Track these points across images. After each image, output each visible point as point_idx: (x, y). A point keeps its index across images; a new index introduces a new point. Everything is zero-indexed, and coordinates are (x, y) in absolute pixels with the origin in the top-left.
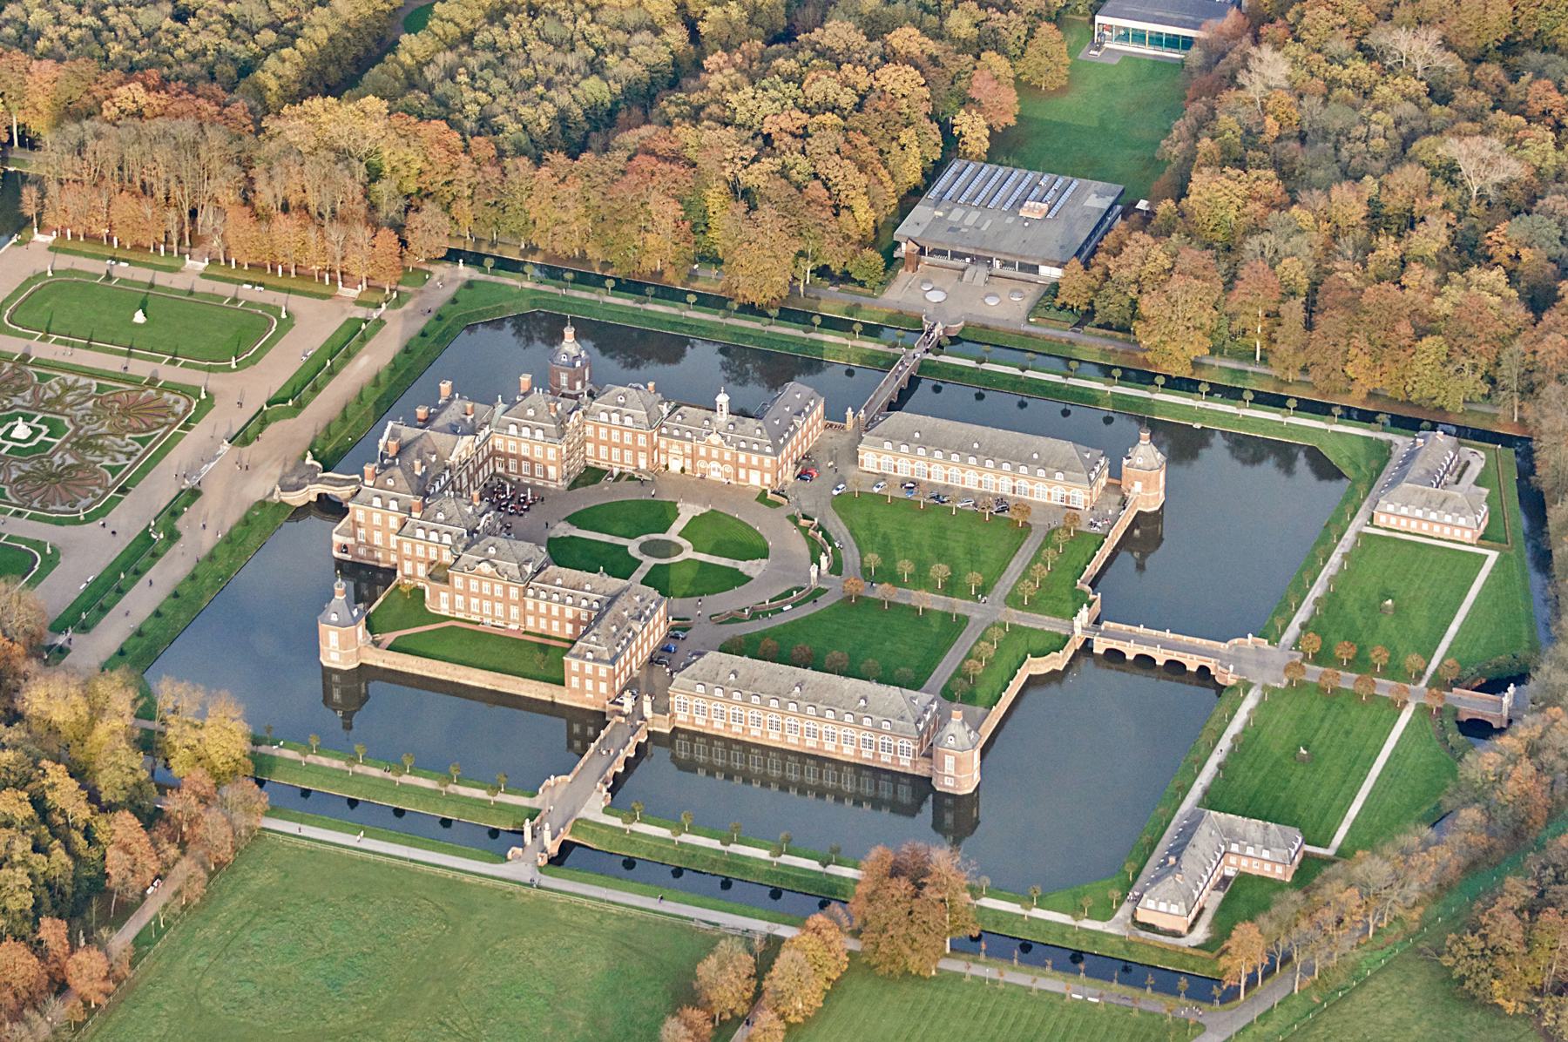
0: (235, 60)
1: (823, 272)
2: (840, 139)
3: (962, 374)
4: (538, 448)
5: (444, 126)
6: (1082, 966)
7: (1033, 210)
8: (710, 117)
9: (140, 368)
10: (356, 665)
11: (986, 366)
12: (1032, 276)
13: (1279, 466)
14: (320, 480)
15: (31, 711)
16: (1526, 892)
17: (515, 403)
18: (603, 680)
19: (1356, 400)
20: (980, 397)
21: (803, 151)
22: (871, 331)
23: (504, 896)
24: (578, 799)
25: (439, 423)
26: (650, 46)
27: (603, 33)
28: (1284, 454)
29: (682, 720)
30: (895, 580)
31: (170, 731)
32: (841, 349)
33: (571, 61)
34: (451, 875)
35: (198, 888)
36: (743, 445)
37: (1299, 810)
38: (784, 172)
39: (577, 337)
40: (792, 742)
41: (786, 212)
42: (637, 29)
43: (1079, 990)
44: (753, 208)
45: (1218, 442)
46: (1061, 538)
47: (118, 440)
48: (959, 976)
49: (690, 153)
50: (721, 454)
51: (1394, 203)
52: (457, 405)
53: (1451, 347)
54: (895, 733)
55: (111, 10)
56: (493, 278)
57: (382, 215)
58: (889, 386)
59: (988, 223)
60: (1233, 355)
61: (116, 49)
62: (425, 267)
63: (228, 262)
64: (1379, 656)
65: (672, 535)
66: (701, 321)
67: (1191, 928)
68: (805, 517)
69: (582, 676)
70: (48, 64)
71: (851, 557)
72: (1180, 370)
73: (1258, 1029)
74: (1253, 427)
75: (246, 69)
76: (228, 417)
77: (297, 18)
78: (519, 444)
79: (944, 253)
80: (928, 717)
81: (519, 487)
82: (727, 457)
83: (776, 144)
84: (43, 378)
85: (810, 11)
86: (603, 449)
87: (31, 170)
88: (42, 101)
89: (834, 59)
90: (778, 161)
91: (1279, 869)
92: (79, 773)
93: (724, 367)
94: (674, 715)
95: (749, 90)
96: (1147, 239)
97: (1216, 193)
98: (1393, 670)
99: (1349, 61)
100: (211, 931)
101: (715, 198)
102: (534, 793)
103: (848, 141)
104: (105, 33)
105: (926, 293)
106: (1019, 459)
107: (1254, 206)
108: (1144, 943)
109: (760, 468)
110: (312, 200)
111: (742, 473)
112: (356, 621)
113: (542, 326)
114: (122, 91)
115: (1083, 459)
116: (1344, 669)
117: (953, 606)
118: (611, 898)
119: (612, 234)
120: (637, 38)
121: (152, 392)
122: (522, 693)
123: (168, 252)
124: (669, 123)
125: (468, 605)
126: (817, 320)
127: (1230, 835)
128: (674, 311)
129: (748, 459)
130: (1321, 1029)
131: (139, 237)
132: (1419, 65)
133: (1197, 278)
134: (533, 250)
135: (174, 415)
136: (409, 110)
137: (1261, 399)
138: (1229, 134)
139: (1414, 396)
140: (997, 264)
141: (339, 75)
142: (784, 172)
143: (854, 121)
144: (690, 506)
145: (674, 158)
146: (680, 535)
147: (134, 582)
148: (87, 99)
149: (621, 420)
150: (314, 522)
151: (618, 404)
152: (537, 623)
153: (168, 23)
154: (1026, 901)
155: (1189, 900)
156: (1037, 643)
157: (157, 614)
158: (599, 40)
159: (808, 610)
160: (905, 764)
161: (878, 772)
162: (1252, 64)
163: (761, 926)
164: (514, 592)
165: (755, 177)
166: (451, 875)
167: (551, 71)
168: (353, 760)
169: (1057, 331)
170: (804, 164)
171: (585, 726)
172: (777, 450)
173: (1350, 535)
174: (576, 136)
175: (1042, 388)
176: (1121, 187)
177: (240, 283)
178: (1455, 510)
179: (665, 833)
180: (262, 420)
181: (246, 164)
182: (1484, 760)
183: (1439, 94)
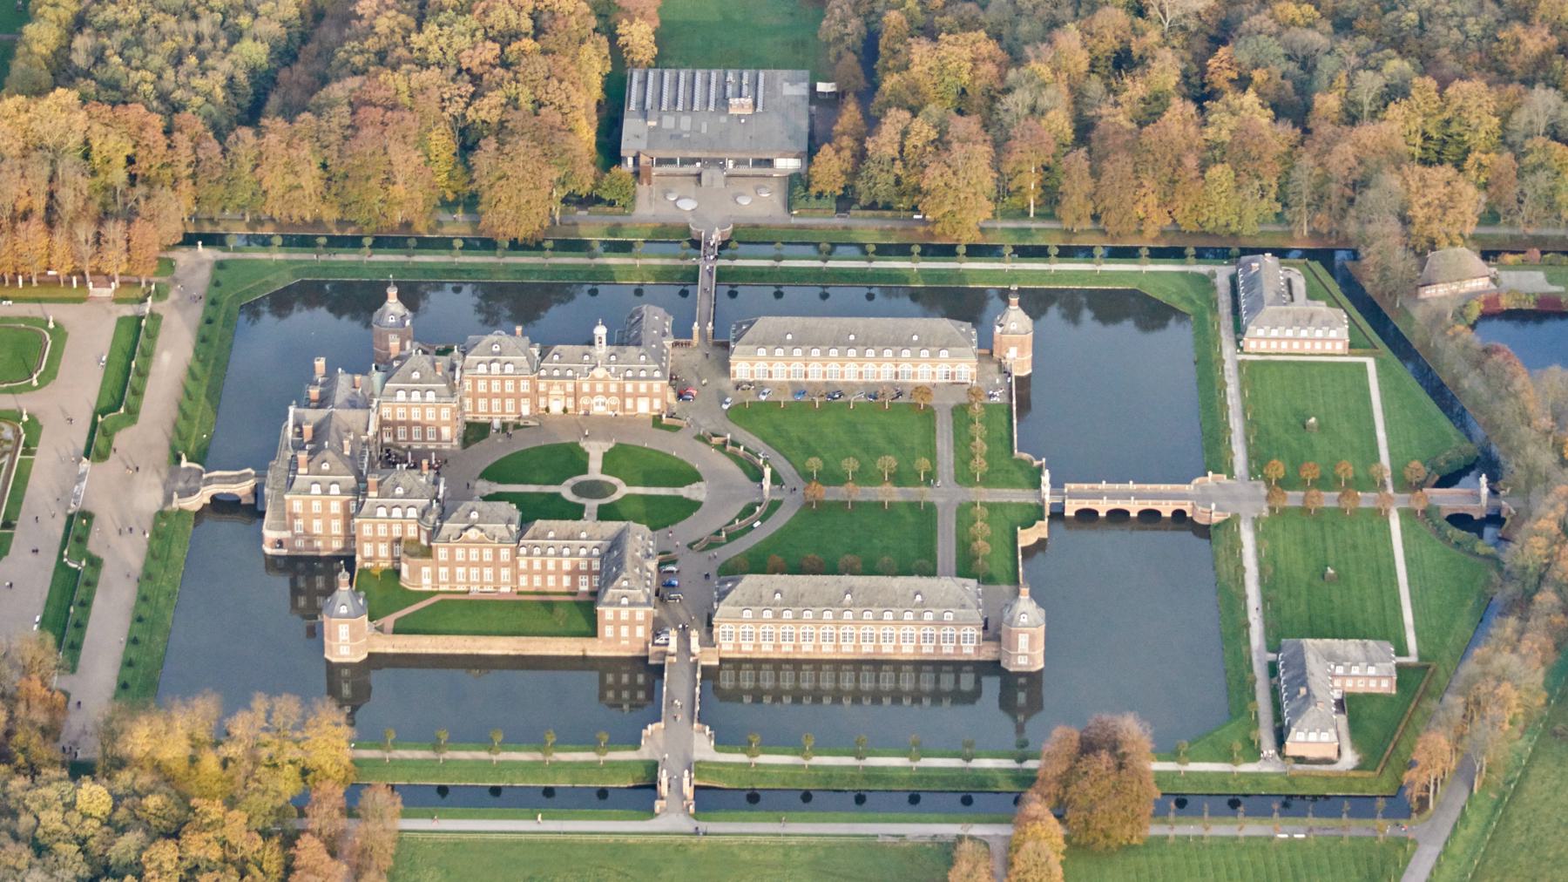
3: (762, 275)
6: (1241, 809)
7: (740, 106)
11: (785, 263)
13: (1064, 316)
14: (209, 482)
15: (138, 752)
20: (779, 295)
23: (673, 851)
24: (680, 745)
29: (727, 648)
32: (630, 270)
33: (205, 26)
34: (612, 839)
37: (1359, 625)
38: (513, 103)
39: (400, 297)
40: (848, 650)
43: (1285, 831)
49: (404, 98)
50: (606, 387)
51: (1109, 44)
52: (343, 379)
54: (957, 624)
56: (239, 255)
60: (1006, 215)
62: (163, 255)
64: (1346, 469)
69: (617, 623)
72: (970, 237)
73: (1463, 832)
74: (1069, 281)
78: (409, 409)
79: (672, 161)
86: (482, 402)
98: (1356, 484)
102: (636, 744)
106: (900, 343)
109: (650, 395)
111: (629, 403)
127: (1332, 657)
129: (636, 388)
130: (1517, 823)
135: (9, 442)
137: (1066, 253)
140: (730, 164)
142: (513, 103)
143: (549, 40)
144: (593, 443)
145: (394, 107)
147: (87, 615)
151: (493, 354)
152: (530, 581)
154: (1174, 756)
157: (134, 641)
160: (969, 651)
161: (938, 666)
164: (505, 554)
165: (488, 109)
169: (826, 220)
176: (807, 73)
178: (1325, 323)
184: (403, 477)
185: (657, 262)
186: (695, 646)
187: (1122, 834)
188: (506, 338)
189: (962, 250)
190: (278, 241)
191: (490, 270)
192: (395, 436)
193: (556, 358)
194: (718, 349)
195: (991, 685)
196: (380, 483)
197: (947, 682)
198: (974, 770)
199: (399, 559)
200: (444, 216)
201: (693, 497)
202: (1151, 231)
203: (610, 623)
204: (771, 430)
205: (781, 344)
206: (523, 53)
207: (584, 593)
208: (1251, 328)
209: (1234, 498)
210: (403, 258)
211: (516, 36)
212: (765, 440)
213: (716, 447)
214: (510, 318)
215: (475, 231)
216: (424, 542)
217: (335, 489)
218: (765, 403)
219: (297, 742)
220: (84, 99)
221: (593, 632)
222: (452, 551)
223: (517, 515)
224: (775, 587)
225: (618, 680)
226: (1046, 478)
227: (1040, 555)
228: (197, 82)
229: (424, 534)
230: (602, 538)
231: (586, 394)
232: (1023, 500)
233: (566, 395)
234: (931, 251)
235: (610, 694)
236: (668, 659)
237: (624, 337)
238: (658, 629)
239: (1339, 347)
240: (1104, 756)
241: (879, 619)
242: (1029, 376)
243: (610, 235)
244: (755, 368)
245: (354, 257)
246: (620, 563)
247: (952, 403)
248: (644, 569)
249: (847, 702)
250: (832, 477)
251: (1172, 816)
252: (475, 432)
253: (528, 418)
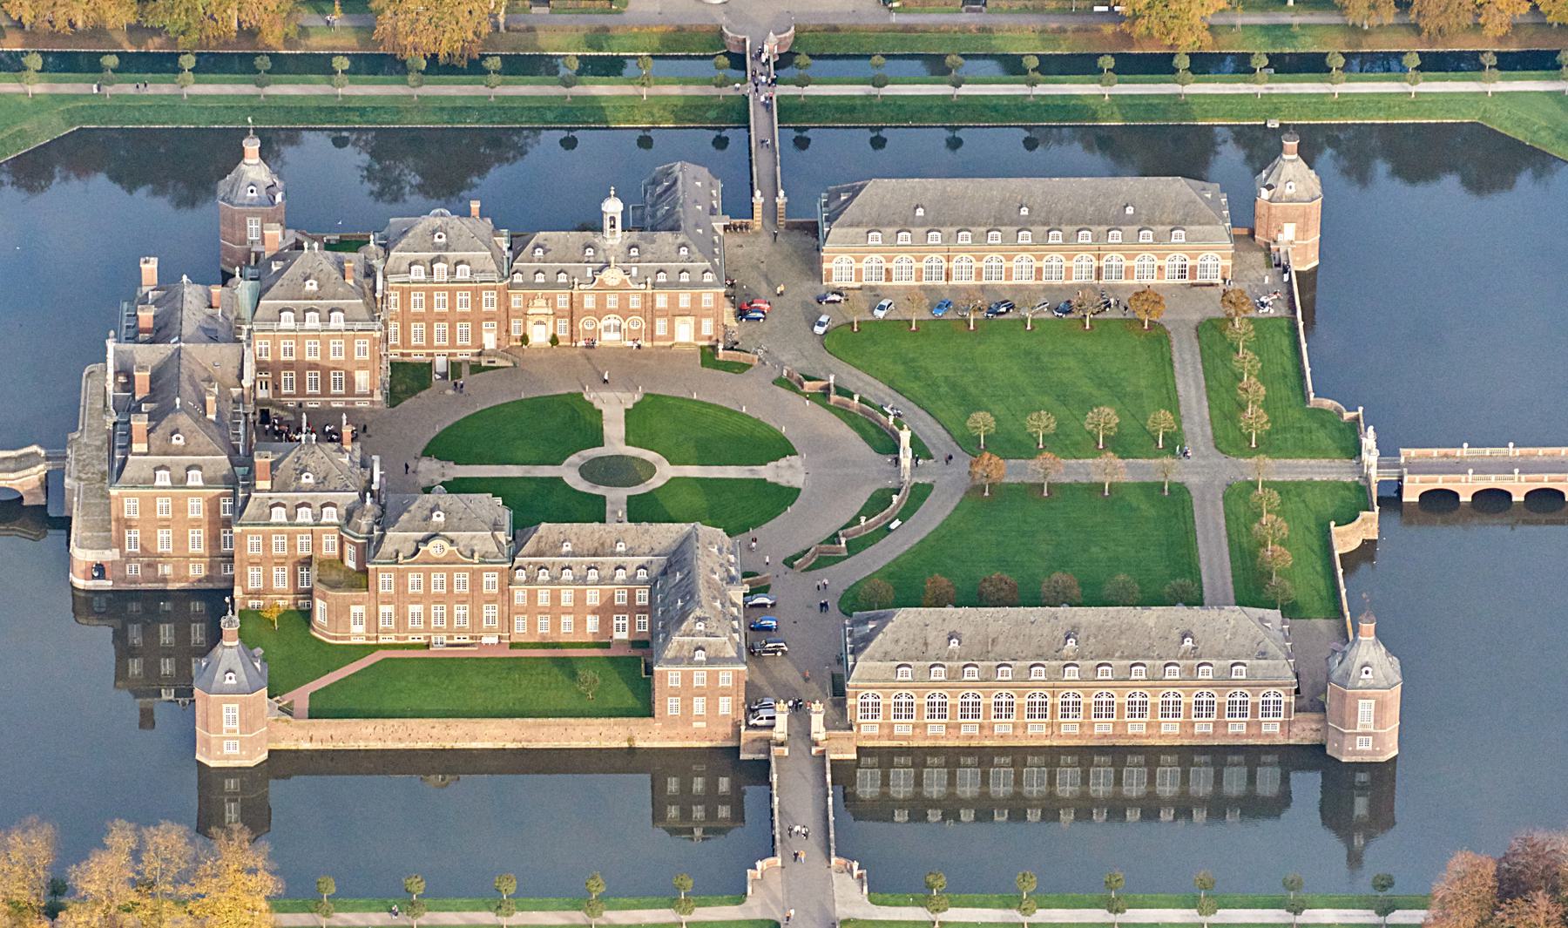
3: (852, 109)
4: (334, 344)
10: (265, 756)
11: (890, 90)
13: (1346, 172)
20: (878, 143)
25: (188, 328)
29: (870, 732)
32: (632, 104)
40: (1070, 732)
50: (624, 300)
52: (192, 294)
54: (1253, 684)
65: (615, 441)
68: (809, 379)
72: (1189, 41)
86: (417, 328)
109: (695, 312)
111: (661, 326)
122: (574, 744)
125: (401, 619)
129: (673, 301)
151: (437, 248)
152: (532, 625)
160: (1272, 730)
161: (1219, 755)
164: (491, 580)
175: (995, 108)
184: (316, 456)
185: (675, 90)
188: (455, 220)
189: (1183, 62)
190: (35, 62)
191: (396, 107)
192: (277, 387)
193: (539, 253)
194: (797, 237)
195: (1307, 786)
196: (274, 466)
197: (1235, 782)
199: (309, 593)
200: (308, 17)
201: (783, 482)
202: (1496, 25)
203: (675, 693)
204: (900, 368)
205: (906, 224)
207: (621, 642)
210: (249, 89)
213: (812, 397)
214: (421, 188)
215: (364, 43)
216: (351, 564)
217: (195, 478)
218: (884, 320)
219: (181, 902)
221: (645, 709)
222: (401, 577)
223: (506, 516)
224: (951, 627)
225: (686, 786)
226: (1369, 440)
227: (1364, 567)
229: (350, 550)
230: (651, 552)
231: (589, 312)
232: (1333, 477)
234: (1130, 66)
235: (673, 812)
236: (775, 751)
237: (653, 214)
238: (753, 703)
240: (1542, 900)
242: (1315, 270)
243: (591, 47)
244: (863, 265)
245: (166, 89)
246: (688, 593)
247: (1196, 317)
248: (728, 602)
249: (1067, 817)
252: (408, 379)
253: (494, 353)
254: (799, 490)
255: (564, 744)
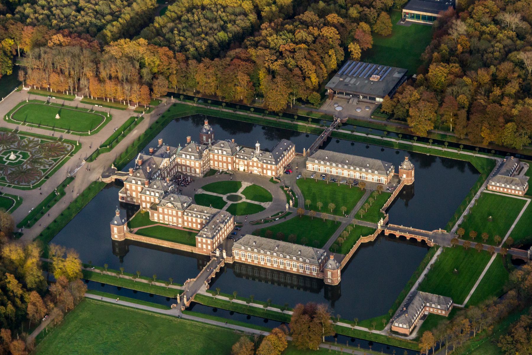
0: (96, 26)
1: (299, 100)
2: (306, 53)
4: (192, 163)
5: (167, 49)
7: (375, 78)
8: (261, 46)
9: (57, 135)
10: (123, 239)
12: (373, 101)
14: (116, 174)
15: (5, 255)
16: (528, 321)
17: (185, 146)
18: (209, 245)
19: (485, 145)
20: (353, 144)
21: (293, 58)
22: (315, 121)
23: (168, 322)
24: (199, 287)
25: (157, 153)
26: (243, 21)
27: (227, 16)
28: (460, 165)
30: (316, 209)
31: (54, 263)
33: (215, 26)
34: (150, 314)
35: (60, 318)
36: (265, 161)
38: (286, 65)
39: (209, 123)
41: (285, 79)
42: (240, 14)
44: (274, 77)
45: (438, 160)
46: (375, 194)
47: (46, 160)
48: (327, 350)
49: (253, 58)
50: (257, 164)
51: (501, 75)
52: (163, 148)
53: (518, 126)
54: (311, 263)
55: (54, 9)
57: (144, 80)
58: (319, 141)
59: (358, 83)
60: (443, 129)
61: (55, 22)
62: (160, 99)
63: (90, 97)
64: (485, 236)
66: (255, 117)
67: (411, 333)
68: (286, 187)
69: (202, 243)
70: (30, 27)
71: (301, 201)
72: (423, 135)
75: (100, 28)
76: (85, 152)
77: (120, 11)
78: (186, 161)
79: (342, 93)
80: (323, 258)
81: (186, 176)
82: (259, 165)
83: (284, 55)
84: (22, 138)
85: (301, 8)
86: (216, 163)
87: (22, 65)
88: (28, 41)
89: (306, 25)
90: (283, 61)
91: (444, 312)
92: (21, 278)
93: (265, 134)
94: (234, 257)
95: (275, 36)
96: (412, 88)
97: (438, 72)
98: (490, 241)
99: (489, 25)
100: (64, 334)
101: (262, 74)
102: (182, 285)
103: (309, 54)
104: (51, 17)
105: (336, 107)
106: (362, 166)
107: (450, 77)
108: (394, 339)
109: (271, 169)
110: (120, 75)
111: (265, 171)
112: (123, 224)
113: (198, 119)
114: (55, 37)
115: (385, 166)
116: (473, 241)
117: (335, 218)
118: (206, 322)
119: (225, 87)
120: (239, 18)
121: (60, 143)
122: (182, 249)
123: (70, 93)
124: (247, 48)
125: (164, 218)
126: (296, 117)
127: (426, 300)
128: (246, 114)
129: (267, 166)
131: (60, 88)
132: (514, 26)
133: (429, 102)
134: (198, 92)
135: (67, 151)
136: (155, 44)
137: (451, 145)
138: (444, 51)
139: (505, 144)
140: (361, 97)
141: (131, 32)
146: (242, 193)
148: (43, 40)
149: (222, 153)
150: (114, 188)
151: (221, 147)
152: (188, 224)
153: (73, 13)
154: (353, 324)
155: (410, 323)
156: (364, 231)
157: (55, 221)
158: (225, 18)
159: (283, 220)
160: (314, 274)
162: (453, 26)
163: (258, 332)
164: (180, 213)
165: (276, 66)
166: (150, 314)
167: (208, 29)
168: (119, 273)
170: (293, 62)
171: (202, 260)
172: (277, 163)
173: (479, 193)
174: (215, 52)
176: (406, 70)
177: (94, 104)
179: (227, 299)
180: (98, 152)
181: (96, 62)
182: (517, 274)
183: (520, 36)
186: (224, 254)
187: (311, 345)
192: (182, 169)
193: (243, 152)
198: (285, 314)
201: (264, 206)
205: (324, 160)
206: (300, 49)
208: (490, 181)
209: (444, 239)
211: (305, 42)
212: (302, 192)
217: (139, 183)
220: (149, 44)
221: (194, 245)
228: (197, 44)
231: (251, 166)
233: (245, 165)
239: (520, 193)
241: (285, 257)
243: (307, 115)
244: (314, 167)
250: (313, 207)
251: (336, 343)
253: (230, 171)
254: (265, 209)
255: (179, 249)
